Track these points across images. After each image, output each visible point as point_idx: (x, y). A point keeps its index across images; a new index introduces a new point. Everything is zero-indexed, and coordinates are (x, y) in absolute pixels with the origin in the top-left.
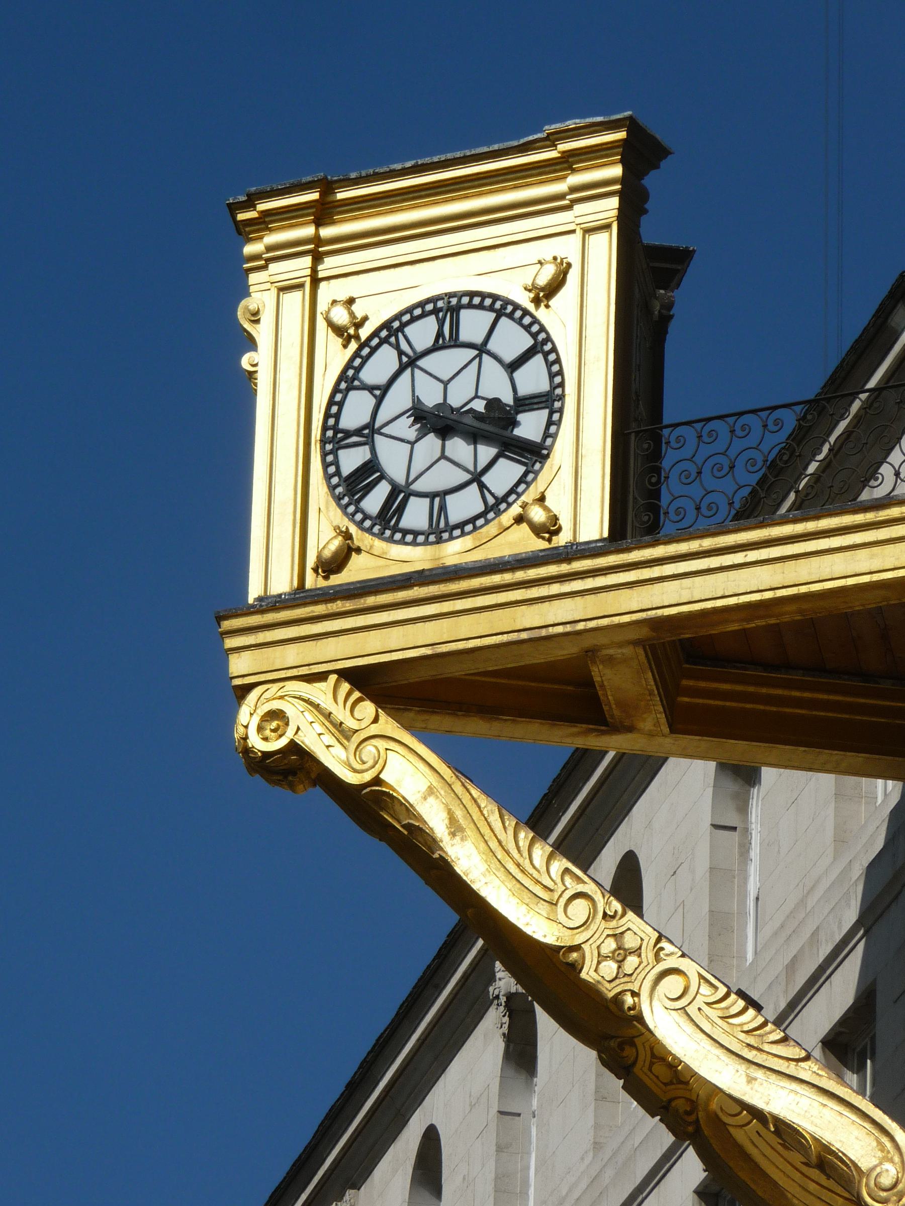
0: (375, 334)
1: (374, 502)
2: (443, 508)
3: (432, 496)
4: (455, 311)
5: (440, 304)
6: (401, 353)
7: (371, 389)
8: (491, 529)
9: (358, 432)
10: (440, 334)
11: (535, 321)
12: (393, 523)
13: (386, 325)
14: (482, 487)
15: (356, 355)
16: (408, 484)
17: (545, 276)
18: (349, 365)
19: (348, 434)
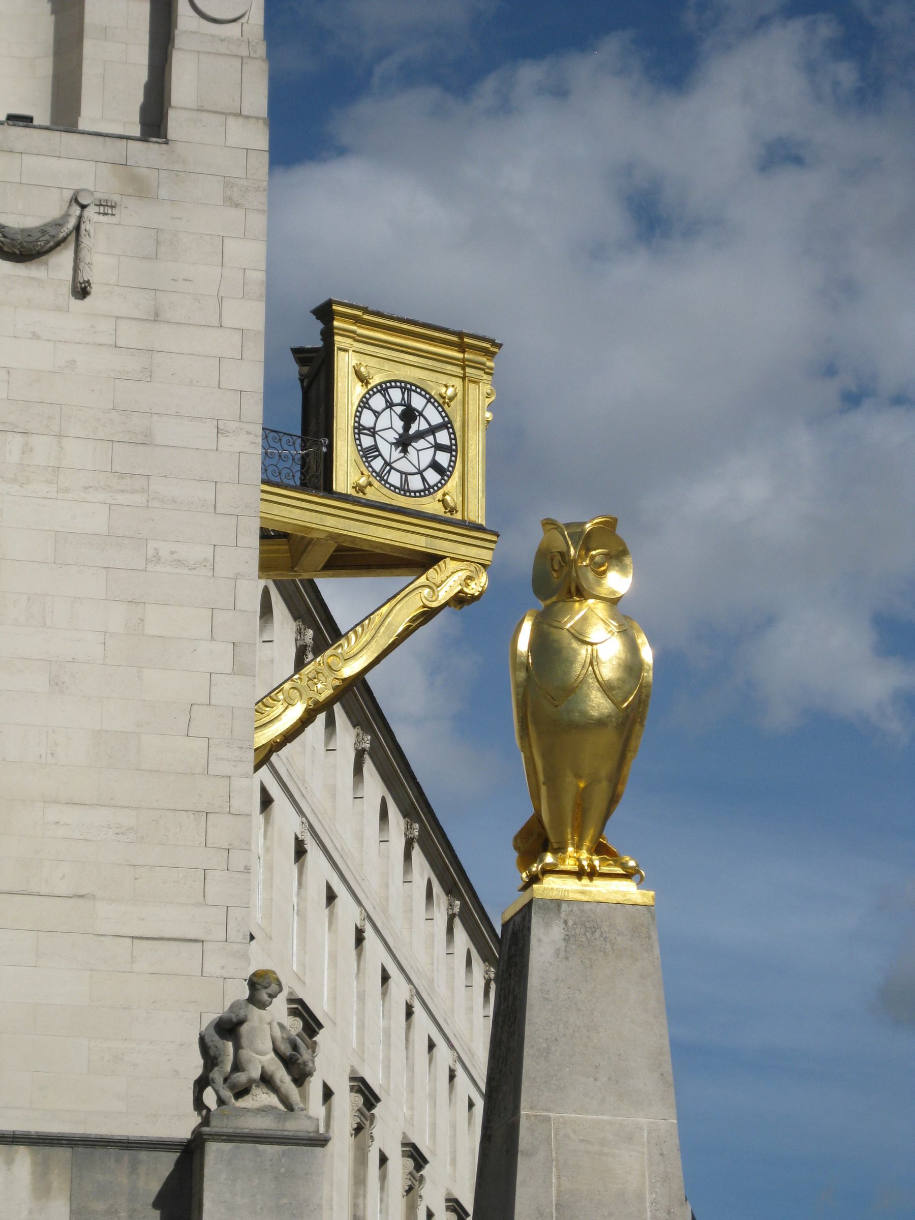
0: (376, 386)
1: (378, 464)
2: (406, 480)
3: (401, 473)
4: (410, 390)
5: (403, 384)
6: (387, 401)
7: (374, 412)
8: (428, 498)
9: (369, 429)
10: (403, 398)
11: (444, 411)
12: (385, 478)
13: (380, 384)
14: (424, 479)
15: (368, 393)
16: (419, 470)
17: (450, 392)
18: (364, 397)
19: (365, 428)
